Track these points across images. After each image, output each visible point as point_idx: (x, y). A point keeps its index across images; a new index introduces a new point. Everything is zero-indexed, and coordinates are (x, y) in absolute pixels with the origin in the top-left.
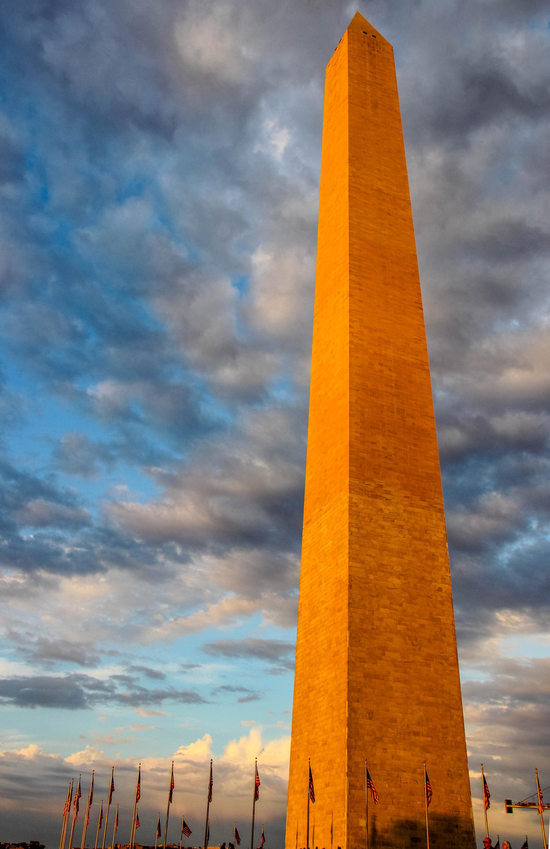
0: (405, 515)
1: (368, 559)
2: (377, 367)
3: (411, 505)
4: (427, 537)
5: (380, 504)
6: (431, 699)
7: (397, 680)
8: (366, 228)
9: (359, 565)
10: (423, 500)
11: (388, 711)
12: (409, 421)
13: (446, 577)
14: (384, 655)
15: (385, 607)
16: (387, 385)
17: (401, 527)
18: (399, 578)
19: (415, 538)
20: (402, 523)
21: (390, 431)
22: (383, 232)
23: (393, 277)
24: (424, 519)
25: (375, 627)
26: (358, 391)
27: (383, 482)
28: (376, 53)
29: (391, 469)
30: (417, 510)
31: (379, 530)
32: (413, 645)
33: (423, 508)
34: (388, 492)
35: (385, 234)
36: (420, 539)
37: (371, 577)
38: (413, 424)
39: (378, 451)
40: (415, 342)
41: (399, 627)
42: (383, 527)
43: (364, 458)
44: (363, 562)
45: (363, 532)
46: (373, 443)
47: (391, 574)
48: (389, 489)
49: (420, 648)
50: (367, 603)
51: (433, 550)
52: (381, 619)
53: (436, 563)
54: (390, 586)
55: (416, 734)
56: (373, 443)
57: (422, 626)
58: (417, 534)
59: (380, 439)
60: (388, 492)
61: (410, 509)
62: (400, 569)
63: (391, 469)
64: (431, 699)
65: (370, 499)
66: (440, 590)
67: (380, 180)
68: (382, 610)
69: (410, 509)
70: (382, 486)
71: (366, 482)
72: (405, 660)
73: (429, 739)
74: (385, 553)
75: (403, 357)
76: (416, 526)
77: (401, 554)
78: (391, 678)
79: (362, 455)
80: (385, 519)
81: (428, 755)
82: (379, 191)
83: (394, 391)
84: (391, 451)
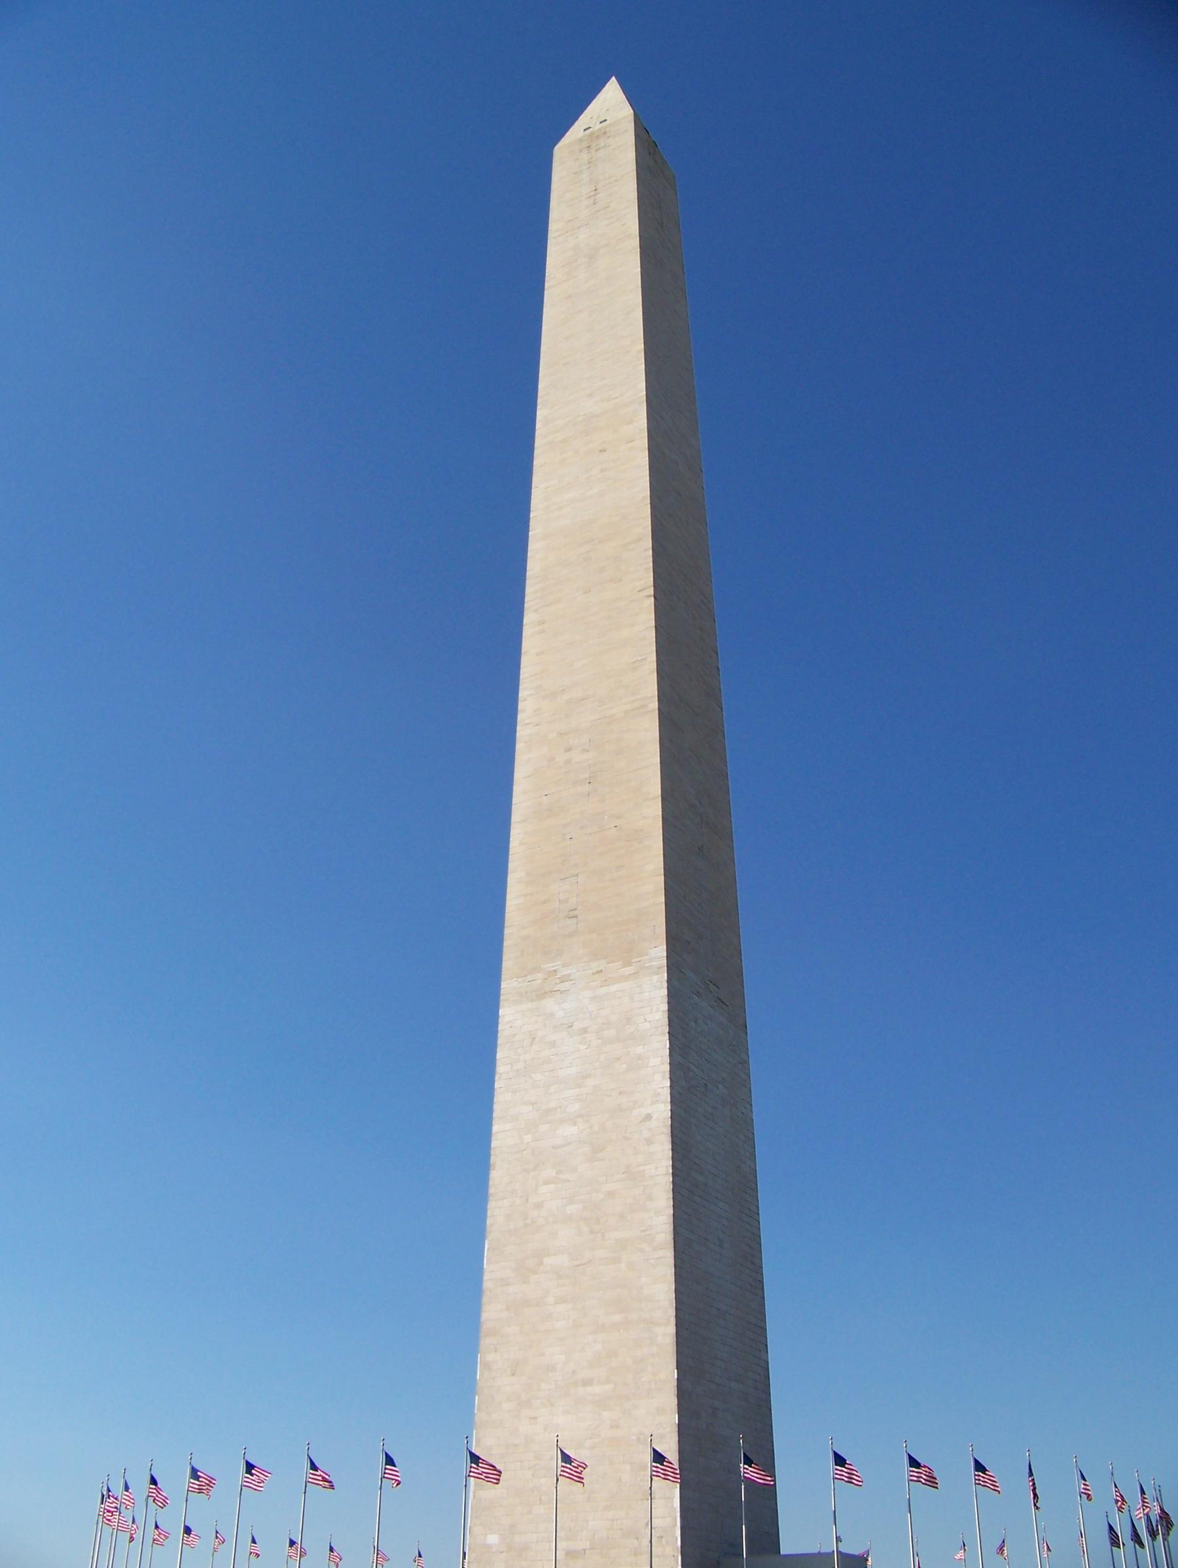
3: (606, 983)
5: (549, 1004)
6: (617, 1318)
7: (561, 1300)
9: (508, 1126)
10: (628, 963)
11: (543, 1355)
13: (660, 1091)
14: (542, 1263)
15: (547, 1183)
17: (585, 1030)
18: (575, 1124)
25: (529, 1221)
26: (525, 821)
28: (601, 154)
32: (592, 1232)
33: (626, 978)
37: (528, 1138)
41: (571, 1209)
42: (553, 1044)
46: (545, 902)
48: (566, 971)
49: (603, 1235)
51: (640, 1050)
52: (539, 1206)
55: (587, 1382)
56: (545, 902)
57: (611, 1194)
60: (563, 980)
61: (604, 990)
62: (577, 1106)
64: (617, 1318)
66: (649, 1117)
67: (590, 395)
68: (543, 1189)
70: (555, 971)
71: (529, 978)
72: (578, 1263)
73: (611, 1386)
78: (551, 1300)
81: (605, 1414)
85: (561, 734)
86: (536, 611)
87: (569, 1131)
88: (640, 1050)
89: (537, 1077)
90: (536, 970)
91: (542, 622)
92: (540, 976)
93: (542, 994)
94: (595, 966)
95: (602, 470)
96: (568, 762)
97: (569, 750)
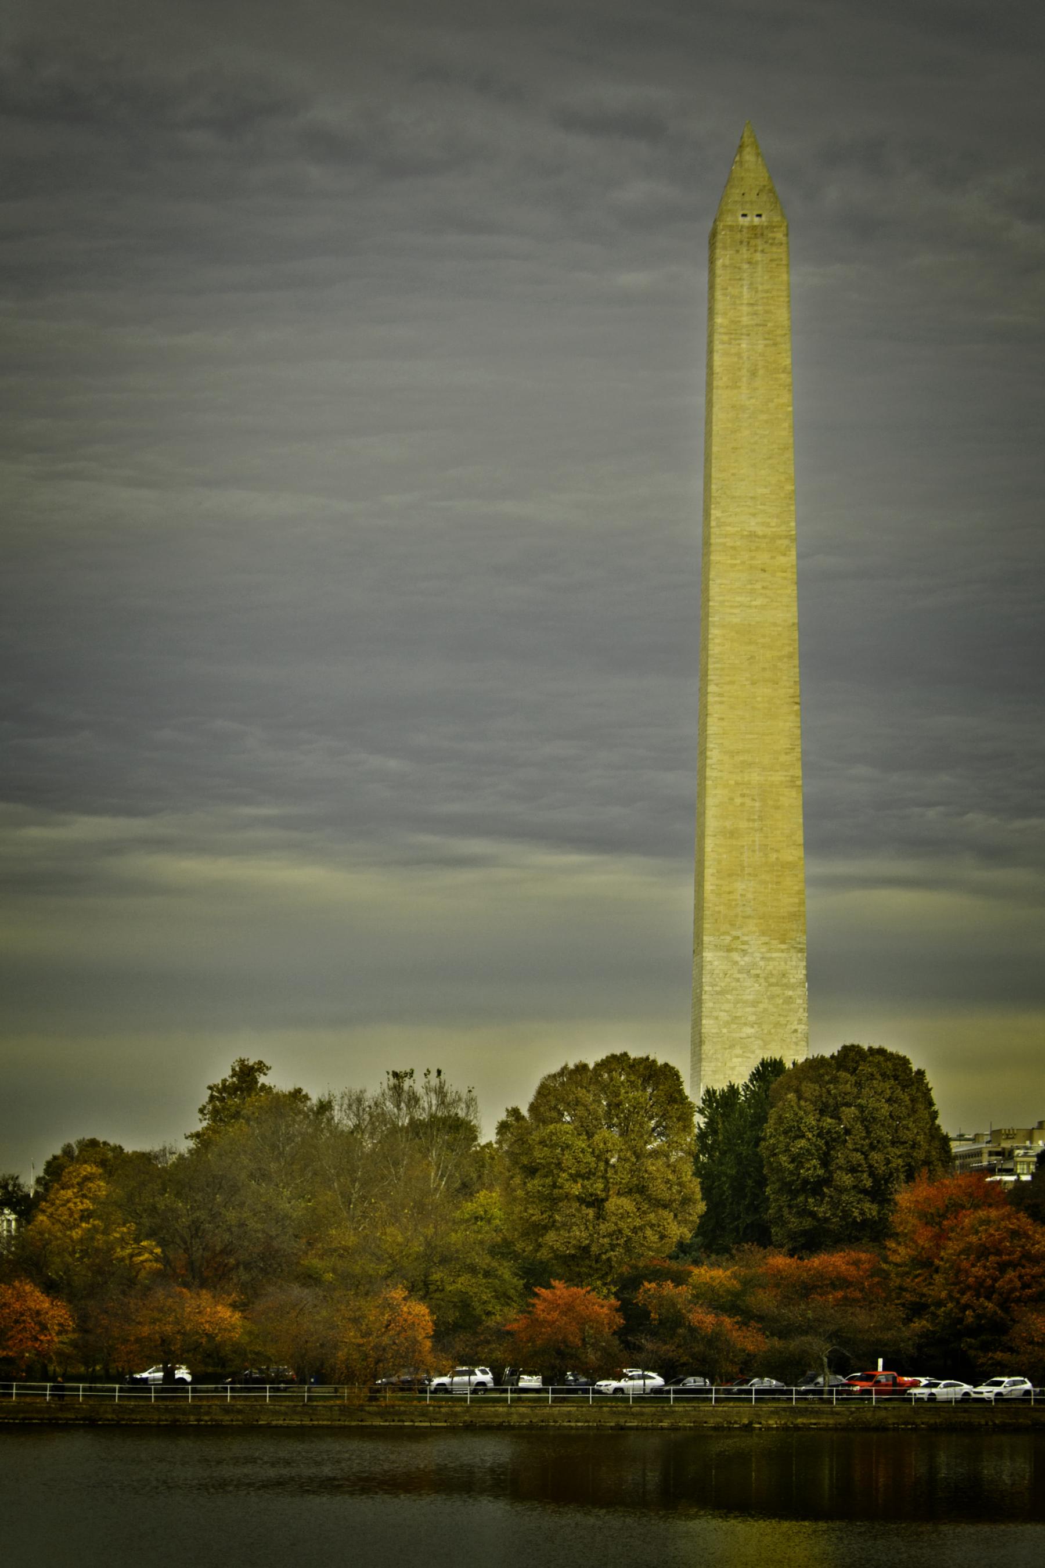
0: (762, 963)
1: (722, 1014)
2: (738, 801)
3: (769, 951)
4: (785, 981)
5: (736, 956)
8: (731, 607)
9: (712, 1022)
10: (783, 942)
12: (773, 856)
15: (737, 1057)
16: (749, 820)
17: (758, 976)
19: (771, 985)
20: (758, 972)
21: (749, 874)
22: (754, 603)
23: (764, 669)
24: (783, 963)
27: (738, 933)
29: (749, 917)
30: (775, 955)
31: (734, 984)
33: (782, 951)
34: (744, 943)
35: (756, 607)
36: (777, 984)
37: (725, 1031)
38: (777, 859)
39: (736, 900)
40: (786, 753)
42: (738, 980)
43: (719, 912)
44: (717, 1018)
45: (718, 989)
47: (745, 1024)
48: (746, 938)
50: (719, 1056)
51: (790, 993)
52: (733, 1068)
53: (793, 1006)
54: (743, 1035)
56: (729, 893)
58: (773, 980)
59: (740, 886)
60: (744, 943)
63: (749, 917)
65: (725, 954)
66: (796, 1031)
67: (754, 515)
68: (735, 1060)
69: (768, 955)
74: (739, 1005)
75: (769, 778)
76: (774, 972)
77: (755, 1004)
79: (717, 909)
80: (739, 972)
82: (753, 535)
83: (756, 825)
84: (750, 896)
85: (737, 784)
86: (717, 685)
87: (749, 1031)
88: (790, 993)
89: (729, 997)
90: (727, 933)
91: (720, 695)
92: (728, 938)
93: (729, 950)
94: (765, 939)
95: (763, 588)
96: (742, 804)
97: (743, 796)
